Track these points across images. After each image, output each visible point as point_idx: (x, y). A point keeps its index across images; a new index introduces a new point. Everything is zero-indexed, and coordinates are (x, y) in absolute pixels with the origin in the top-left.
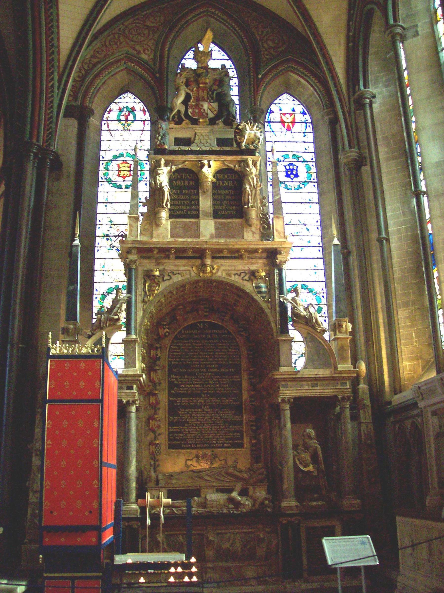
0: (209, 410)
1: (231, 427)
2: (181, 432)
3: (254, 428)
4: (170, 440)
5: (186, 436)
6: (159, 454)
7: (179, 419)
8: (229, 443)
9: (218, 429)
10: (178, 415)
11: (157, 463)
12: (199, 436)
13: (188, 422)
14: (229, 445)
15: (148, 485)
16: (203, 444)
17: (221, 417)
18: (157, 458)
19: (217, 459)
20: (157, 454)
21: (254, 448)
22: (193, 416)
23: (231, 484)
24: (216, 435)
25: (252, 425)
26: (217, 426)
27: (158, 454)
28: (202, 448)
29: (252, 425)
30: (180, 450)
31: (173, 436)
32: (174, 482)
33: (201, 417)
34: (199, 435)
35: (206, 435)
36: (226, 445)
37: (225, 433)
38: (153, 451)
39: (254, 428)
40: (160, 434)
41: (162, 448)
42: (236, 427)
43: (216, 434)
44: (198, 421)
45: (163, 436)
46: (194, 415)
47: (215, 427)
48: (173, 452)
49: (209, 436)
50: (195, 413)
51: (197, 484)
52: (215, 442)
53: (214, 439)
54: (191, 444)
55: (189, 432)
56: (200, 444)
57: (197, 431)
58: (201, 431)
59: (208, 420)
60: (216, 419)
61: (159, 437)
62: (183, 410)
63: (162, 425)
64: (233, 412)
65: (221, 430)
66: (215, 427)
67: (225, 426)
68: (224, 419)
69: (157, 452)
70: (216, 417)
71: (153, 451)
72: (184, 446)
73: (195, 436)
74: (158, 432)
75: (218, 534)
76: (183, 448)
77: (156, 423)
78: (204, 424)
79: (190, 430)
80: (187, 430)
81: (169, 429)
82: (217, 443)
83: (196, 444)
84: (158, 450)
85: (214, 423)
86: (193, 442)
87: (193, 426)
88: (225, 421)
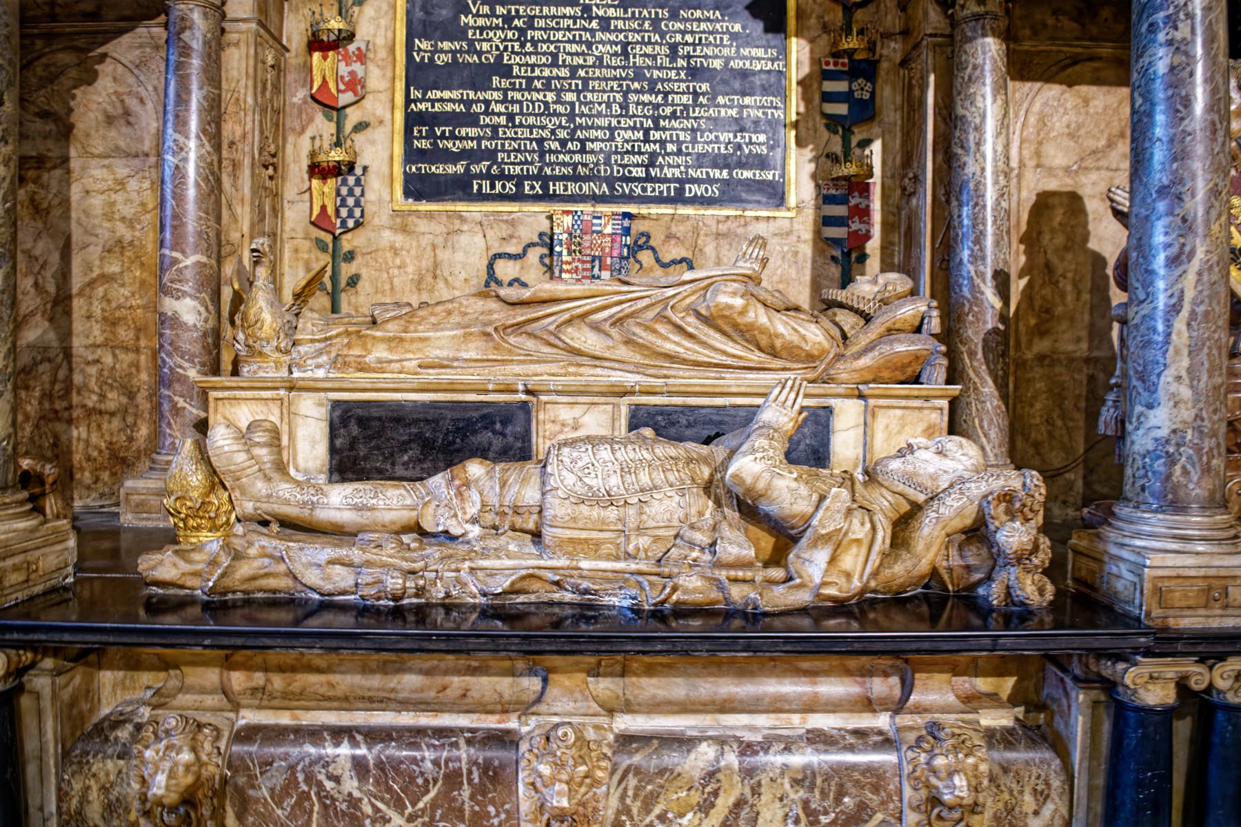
0: (611, 12)
1: (721, 100)
2: (471, 119)
3: (842, 109)
4: (412, 155)
5: (495, 137)
6: (358, 224)
7: (461, 51)
8: (710, 181)
9: (656, 107)
10: (459, 33)
11: (347, 270)
12: (563, 143)
13: (506, 72)
14: (714, 191)
15: (245, 370)
16: (576, 178)
17: (674, 48)
18: (347, 243)
19: (646, 257)
20: (344, 223)
21: (840, 211)
22: (534, 43)
23: (732, 380)
24: (646, 140)
25: (827, 97)
26: (652, 91)
27: (351, 223)
28: (573, 199)
29: (827, 97)
30: (461, 207)
31: (431, 135)
32: (380, 352)
33: (575, 48)
34: (562, 134)
35: (599, 134)
36: (695, 188)
37: (693, 130)
38: (323, 208)
39: (842, 109)
40: (361, 127)
41: (370, 196)
42: (747, 100)
43: (647, 132)
44: (554, 64)
45: (378, 134)
46: (537, 35)
47: (646, 98)
48: (430, 215)
49: (612, 139)
50: (542, 23)
51: (517, 373)
52: (639, 172)
53: (637, 159)
54: (519, 180)
55: (511, 117)
56: (564, 178)
57: (548, 112)
58: (571, 116)
59: (606, 59)
60: (654, 57)
61: (359, 138)
62: (486, 9)
63: (376, 79)
64: (737, 27)
65: (674, 116)
66: (646, 98)
67: (696, 94)
68: (689, 57)
69: (344, 212)
70: (649, 50)
71: (323, 208)
72: (486, 189)
73: (540, 141)
74: (353, 116)
75: (627, 741)
76: (482, 197)
77: (344, 69)
78: (585, 81)
79: (516, 108)
80: (500, 108)
81: (408, 101)
82: (648, 179)
83: (545, 180)
84: (351, 201)
85: (639, 76)
86: (534, 170)
87: (530, 88)
88: (694, 73)
